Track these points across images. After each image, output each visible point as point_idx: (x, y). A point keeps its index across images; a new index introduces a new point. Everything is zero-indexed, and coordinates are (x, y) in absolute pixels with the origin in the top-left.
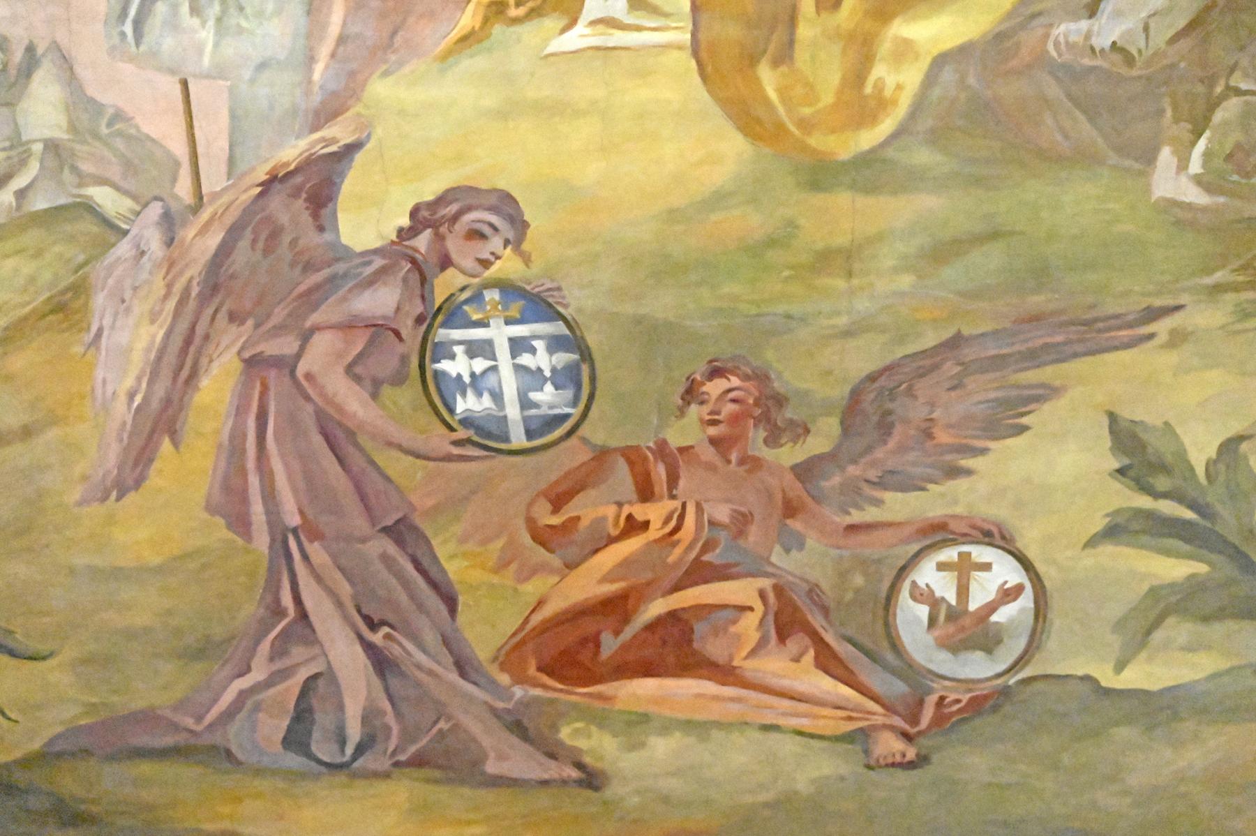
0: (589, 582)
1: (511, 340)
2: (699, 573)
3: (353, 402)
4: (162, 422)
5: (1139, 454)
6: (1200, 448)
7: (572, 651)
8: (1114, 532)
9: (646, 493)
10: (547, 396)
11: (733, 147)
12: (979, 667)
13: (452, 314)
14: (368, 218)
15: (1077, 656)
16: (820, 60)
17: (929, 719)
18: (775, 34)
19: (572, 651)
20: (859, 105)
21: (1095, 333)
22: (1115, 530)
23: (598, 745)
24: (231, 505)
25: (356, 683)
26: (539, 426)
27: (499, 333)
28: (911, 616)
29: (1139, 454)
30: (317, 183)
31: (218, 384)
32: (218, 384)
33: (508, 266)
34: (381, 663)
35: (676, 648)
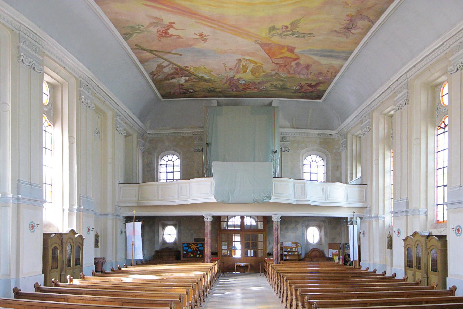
4: (226, 83)
7: (245, 89)
11: (253, 77)
14: (235, 78)
15: (268, 89)
16: (257, 75)
17: (261, 91)
18: (255, 74)
19: (245, 89)
20: (259, 75)
21: (269, 81)
24: (229, 85)
25: (235, 89)
28: (261, 88)
29: (271, 84)
30: (233, 77)
32: (229, 82)
35: (250, 89)
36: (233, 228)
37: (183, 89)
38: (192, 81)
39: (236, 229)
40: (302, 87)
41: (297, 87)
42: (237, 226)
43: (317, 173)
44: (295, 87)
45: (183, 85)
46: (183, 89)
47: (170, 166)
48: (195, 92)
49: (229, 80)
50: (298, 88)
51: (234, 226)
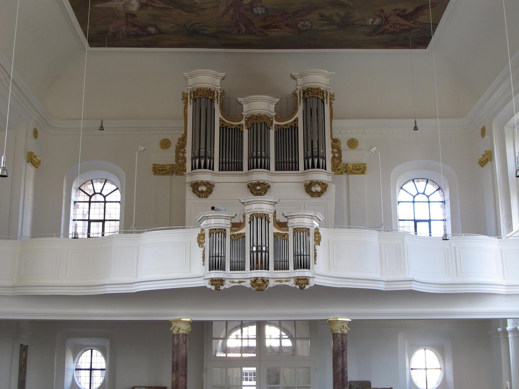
0: (268, 23)
1: (275, 270)
2: (278, 23)
3: (245, 12)
5: (321, 15)
6: (328, 15)
7: (266, 27)
8: (320, 20)
9: (273, 18)
10: (263, 12)
12: (306, 28)
13: (254, 7)
19: (266, 27)
22: (320, 20)
23: (269, 33)
25: (244, 29)
26: (263, 14)
27: (259, 9)
28: (299, 25)
29: (321, 15)
31: (231, 11)
32: (231, 11)
33: (260, 4)
34: (247, 28)
35: (276, 27)
36: (239, 355)
37: (135, 26)
38: (154, 7)
39: (245, 355)
40: (386, 18)
41: (375, 19)
42: (248, 349)
43: (429, 221)
44: (371, 20)
45: (133, 15)
46: (135, 26)
47: (97, 206)
48: (160, 32)
49: (231, 5)
50: (377, 21)
51: (243, 350)
